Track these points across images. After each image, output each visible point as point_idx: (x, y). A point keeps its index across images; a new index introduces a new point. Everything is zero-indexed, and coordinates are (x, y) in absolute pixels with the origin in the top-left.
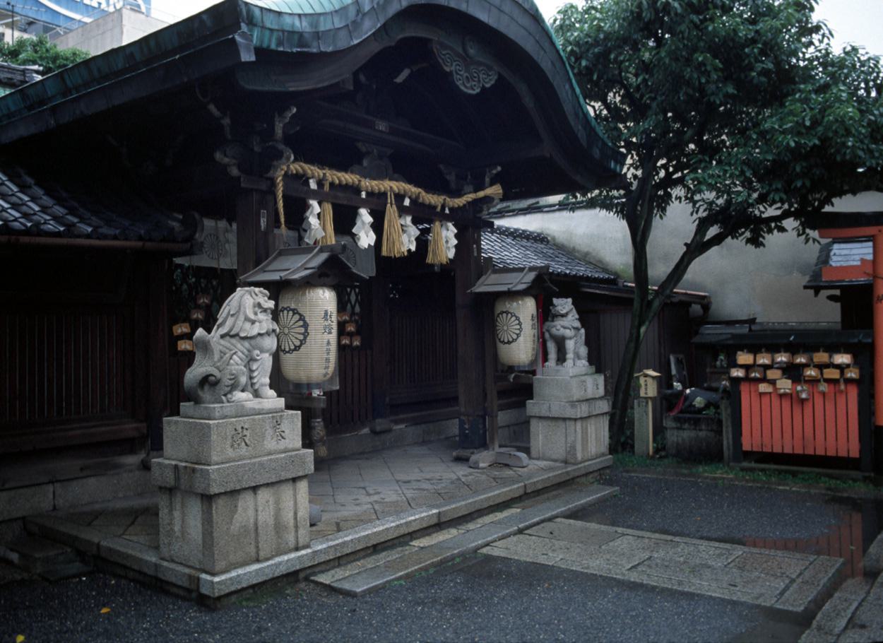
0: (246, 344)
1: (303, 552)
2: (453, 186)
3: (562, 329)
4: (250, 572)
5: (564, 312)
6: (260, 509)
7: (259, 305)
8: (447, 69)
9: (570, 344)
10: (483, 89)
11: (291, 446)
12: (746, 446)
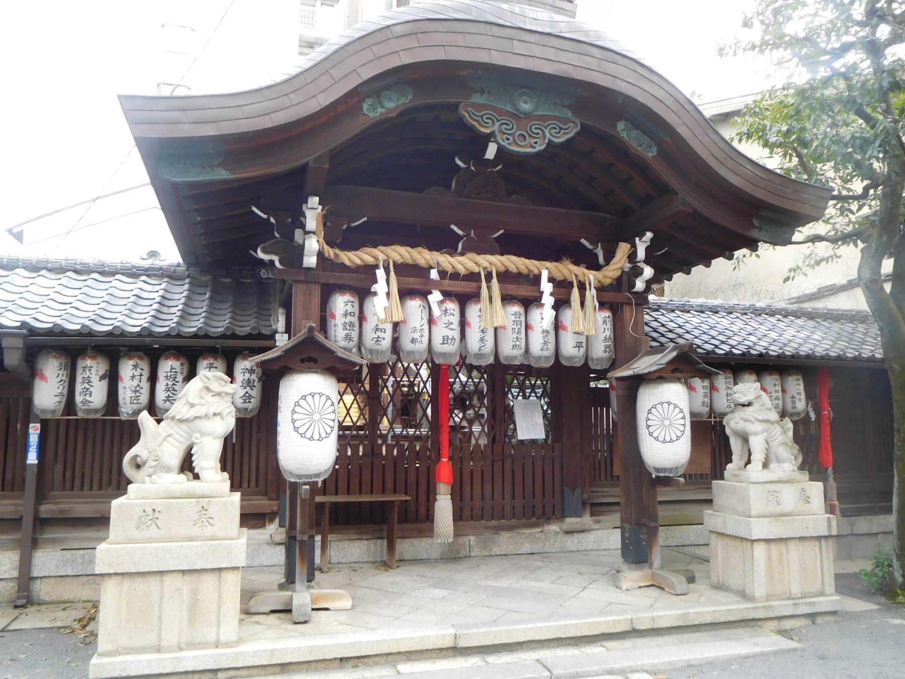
0: (184, 426)
2: (601, 260)
3: (742, 422)
4: (140, 662)
5: (743, 399)
7: (208, 389)
8: (488, 131)
9: (757, 444)
10: (550, 144)
11: (221, 534)
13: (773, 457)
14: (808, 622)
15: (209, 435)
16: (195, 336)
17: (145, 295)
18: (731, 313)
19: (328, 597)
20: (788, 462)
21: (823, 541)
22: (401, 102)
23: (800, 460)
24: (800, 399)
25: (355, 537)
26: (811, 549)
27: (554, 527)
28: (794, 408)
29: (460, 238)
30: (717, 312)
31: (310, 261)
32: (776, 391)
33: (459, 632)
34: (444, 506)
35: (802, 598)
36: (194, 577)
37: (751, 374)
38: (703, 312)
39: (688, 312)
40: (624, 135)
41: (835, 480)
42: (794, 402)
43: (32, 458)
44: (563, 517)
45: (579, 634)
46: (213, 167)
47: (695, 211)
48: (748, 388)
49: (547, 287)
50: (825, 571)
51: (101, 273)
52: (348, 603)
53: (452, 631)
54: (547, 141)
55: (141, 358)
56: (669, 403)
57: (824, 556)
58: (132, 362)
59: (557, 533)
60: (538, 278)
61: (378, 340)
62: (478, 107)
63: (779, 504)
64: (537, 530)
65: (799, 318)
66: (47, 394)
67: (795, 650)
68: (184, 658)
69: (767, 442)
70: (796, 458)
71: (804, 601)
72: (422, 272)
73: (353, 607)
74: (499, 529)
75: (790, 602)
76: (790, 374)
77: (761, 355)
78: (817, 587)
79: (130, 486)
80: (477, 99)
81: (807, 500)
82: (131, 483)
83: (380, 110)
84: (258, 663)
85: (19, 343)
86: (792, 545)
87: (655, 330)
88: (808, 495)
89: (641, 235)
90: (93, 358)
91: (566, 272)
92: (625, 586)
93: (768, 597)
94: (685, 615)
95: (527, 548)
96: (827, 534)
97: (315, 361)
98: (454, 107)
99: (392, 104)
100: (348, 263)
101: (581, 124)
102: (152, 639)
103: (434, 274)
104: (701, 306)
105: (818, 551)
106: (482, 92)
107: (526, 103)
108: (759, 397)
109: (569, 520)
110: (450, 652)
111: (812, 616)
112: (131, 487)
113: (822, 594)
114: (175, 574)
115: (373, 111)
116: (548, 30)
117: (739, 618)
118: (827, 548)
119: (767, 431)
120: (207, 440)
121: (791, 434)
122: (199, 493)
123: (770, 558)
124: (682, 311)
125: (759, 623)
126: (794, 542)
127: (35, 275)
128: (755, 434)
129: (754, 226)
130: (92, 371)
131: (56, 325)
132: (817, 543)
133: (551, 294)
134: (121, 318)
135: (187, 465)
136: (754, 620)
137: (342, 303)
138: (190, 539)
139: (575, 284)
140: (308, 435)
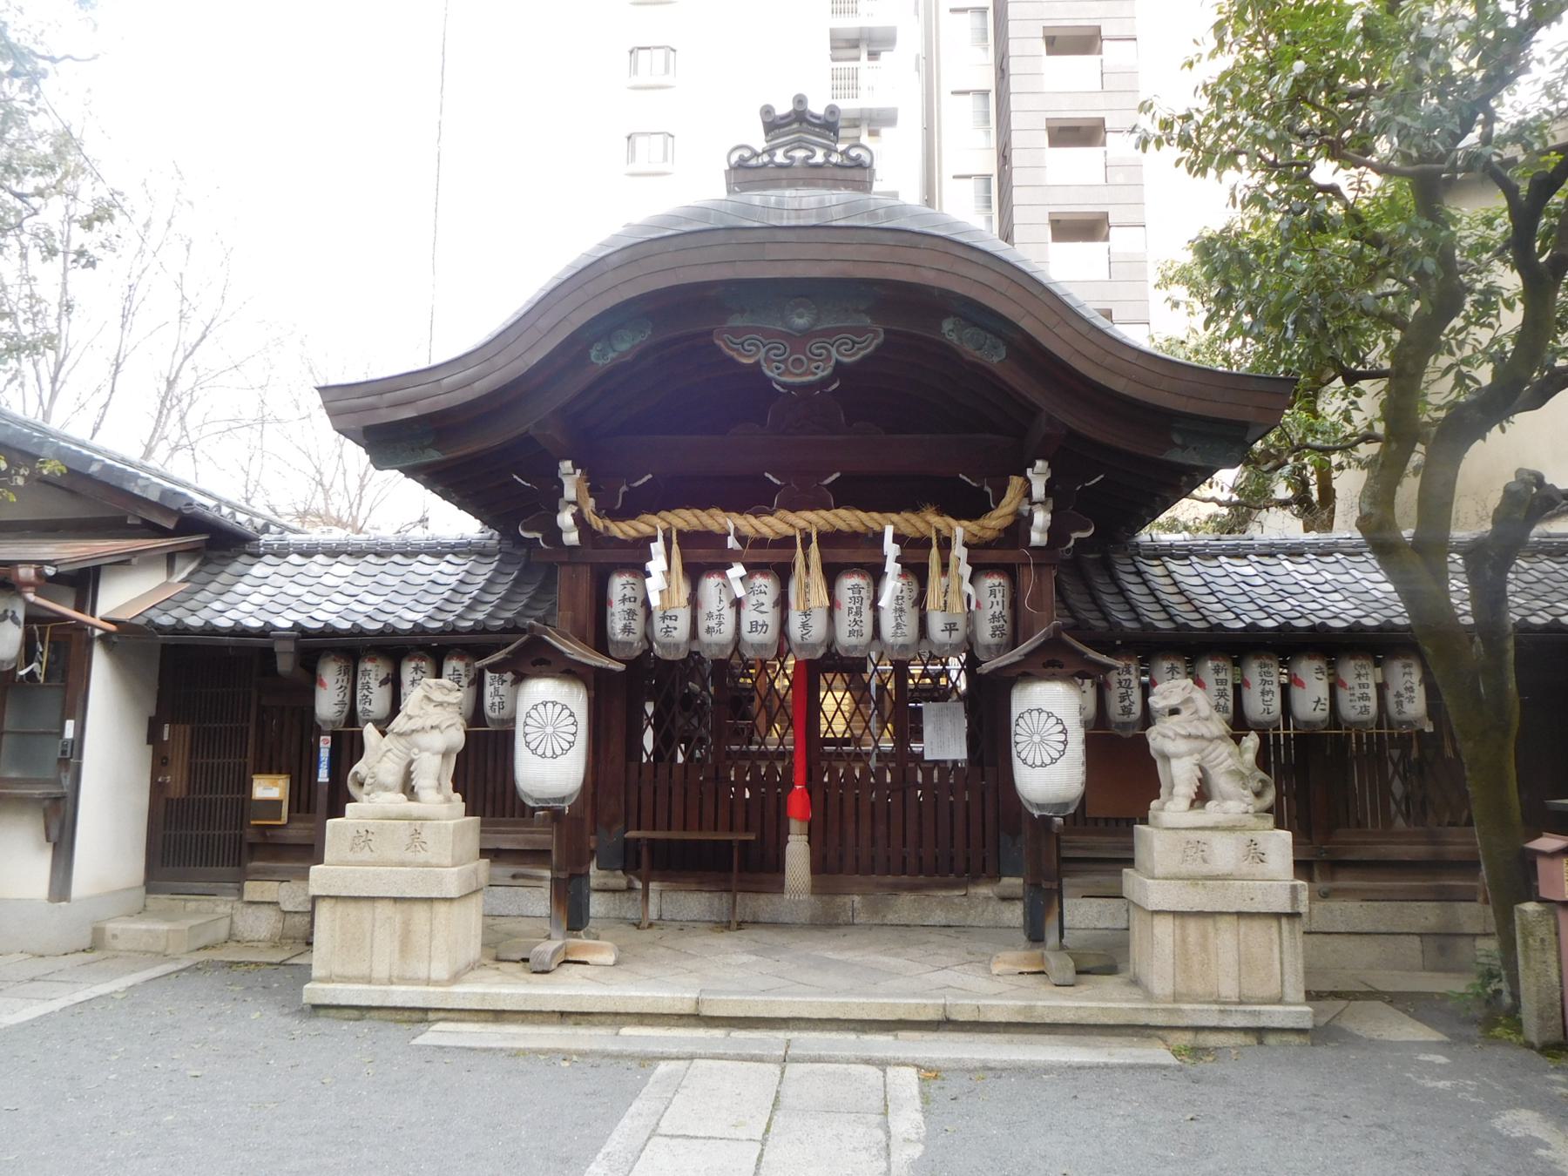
0: (402, 740)
1: (431, 989)
3: (1159, 738)
6: (378, 924)
7: (429, 699)
8: (751, 361)
11: (434, 861)
14: (1251, 1040)
15: (427, 750)
16: (472, 631)
17: (442, 579)
18: (1330, 554)
19: (585, 949)
20: (1236, 802)
21: (1284, 921)
22: (637, 341)
23: (1270, 797)
24: (1411, 700)
25: (694, 887)
27: (984, 890)
28: (1400, 712)
29: (779, 488)
30: (1301, 555)
31: (572, 538)
33: (704, 996)
34: (797, 851)
35: (1241, 1003)
36: (405, 906)
37: (1310, 658)
38: (1272, 555)
39: (1245, 557)
40: (953, 338)
42: (1400, 704)
43: (323, 776)
44: (996, 876)
45: (866, 1017)
46: (423, 449)
47: (1072, 434)
48: (1171, 689)
49: (891, 549)
50: (1286, 965)
51: (404, 554)
52: (610, 958)
53: (695, 996)
54: (832, 363)
55: (422, 659)
56: (1040, 711)
57: (1286, 944)
58: (413, 664)
59: (988, 899)
60: (880, 536)
61: (667, 630)
62: (736, 332)
63: (1205, 861)
64: (957, 893)
66: (328, 703)
68: (393, 992)
69: (1202, 769)
70: (1258, 795)
71: (1241, 1008)
72: (715, 540)
73: (617, 963)
74: (896, 889)
75: (1216, 1007)
78: (1273, 989)
79: (349, 806)
80: (736, 321)
82: (352, 799)
83: (612, 355)
84: (468, 1007)
85: (290, 646)
86: (1225, 924)
87: (1152, 592)
88: (1261, 848)
89: (1032, 465)
90: (373, 660)
91: (921, 526)
92: (996, 969)
93: (1177, 997)
94: (1031, 1008)
95: (939, 917)
97: (548, 663)
98: (710, 333)
99: (625, 345)
100: (621, 536)
101: (886, 332)
102: (363, 969)
103: (732, 543)
104: (1272, 545)
105: (1275, 936)
106: (742, 311)
107: (801, 316)
108: (1188, 700)
109: (1006, 880)
110: (693, 1021)
111: (1260, 1032)
112: (349, 806)
113: (1280, 1001)
114: (386, 902)
115: (601, 358)
116: (813, 222)
117: (1121, 1020)
118: (1292, 932)
119: (1201, 751)
120: (426, 755)
121: (1250, 757)
122: (415, 815)
123: (1184, 941)
124: (1228, 557)
125: (1160, 1033)
126: (1228, 918)
127: (332, 561)
128: (1178, 756)
130: (373, 673)
131: (327, 624)
132: (1274, 924)
133: (898, 560)
134: (401, 611)
135: (408, 788)
136: (1147, 1027)
137: (619, 586)
138: (403, 864)
139: (934, 542)
140: (540, 751)
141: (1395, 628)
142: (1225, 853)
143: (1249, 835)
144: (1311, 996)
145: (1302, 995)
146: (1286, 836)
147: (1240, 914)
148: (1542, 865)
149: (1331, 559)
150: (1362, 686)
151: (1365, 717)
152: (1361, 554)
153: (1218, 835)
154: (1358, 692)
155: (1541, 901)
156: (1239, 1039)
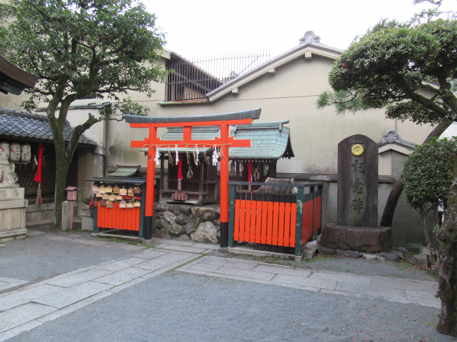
12: (99, 226)
13: (5, 178)
14: (13, 238)
18: (2, 114)
21: (22, 209)
23: (17, 179)
24: (28, 156)
26: (17, 212)
28: (25, 159)
32: (17, 151)
37: (6, 143)
41: (41, 188)
42: (25, 157)
63: (5, 196)
65: (36, 120)
67: (3, 247)
69: (2, 172)
70: (15, 179)
76: (25, 144)
77: (11, 136)
78: (18, 226)
81: (17, 194)
86: (9, 211)
88: (17, 192)
96: (23, 206)
105: (20, 213)
111: (15, 236)
113: (19, 228)
118: (23, 212)
121: (14, 169)
126: (10, 210)
129: (5, 85)
132: (19, 210)
141: (49, 140)
142: (9, 193)
143: (15, 189)
144: (27, 227)
145: (24, 227)
146: (23, 189)
147: (13, 208)
148: (69, 193)
149: (3, 115)
150: (17, 151)
151: (17, 159)
152: (10, 115)
153: (8, 189)
154: (16, 153)
155: (69, 201)
156: (10, 239)
